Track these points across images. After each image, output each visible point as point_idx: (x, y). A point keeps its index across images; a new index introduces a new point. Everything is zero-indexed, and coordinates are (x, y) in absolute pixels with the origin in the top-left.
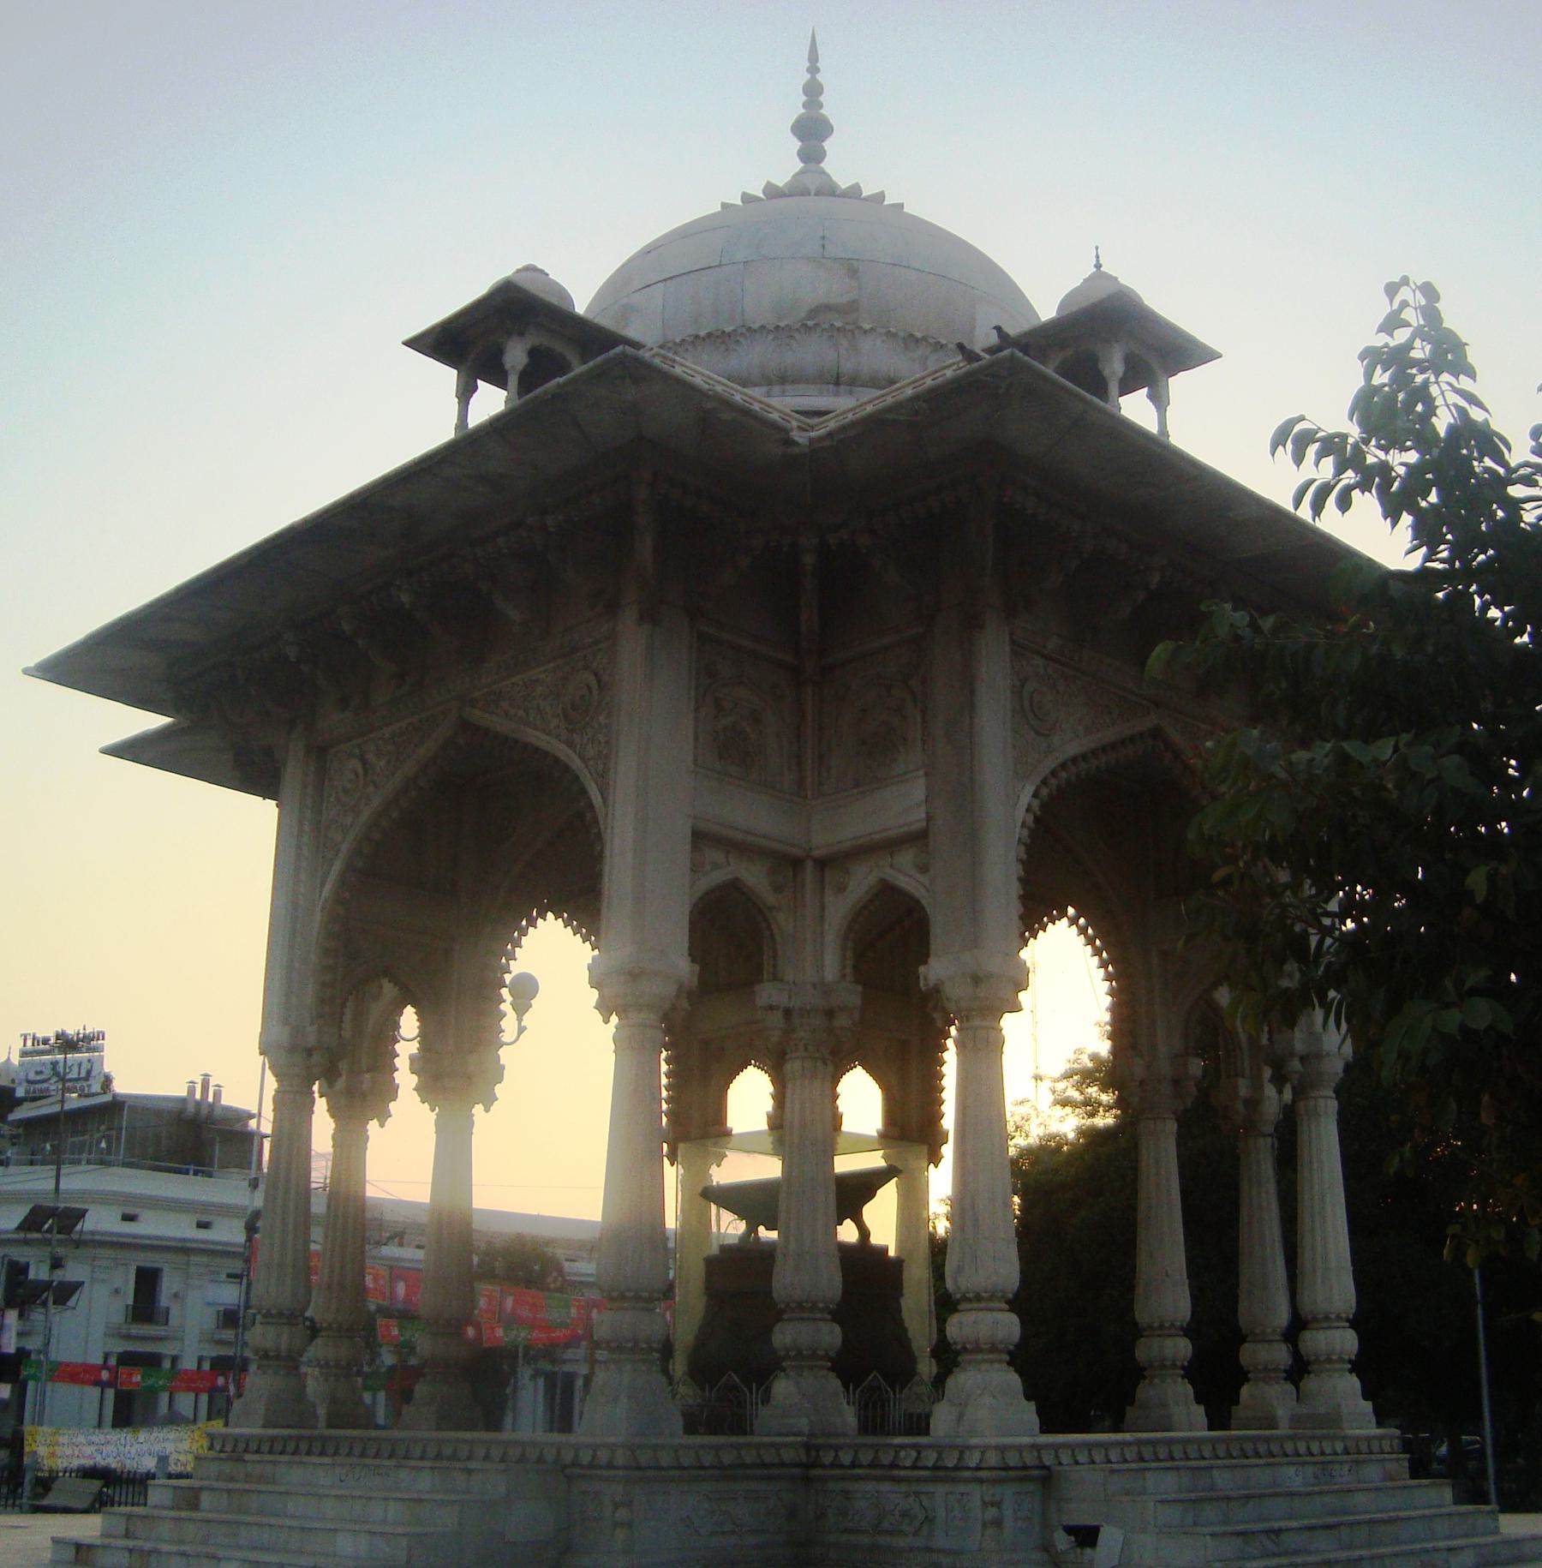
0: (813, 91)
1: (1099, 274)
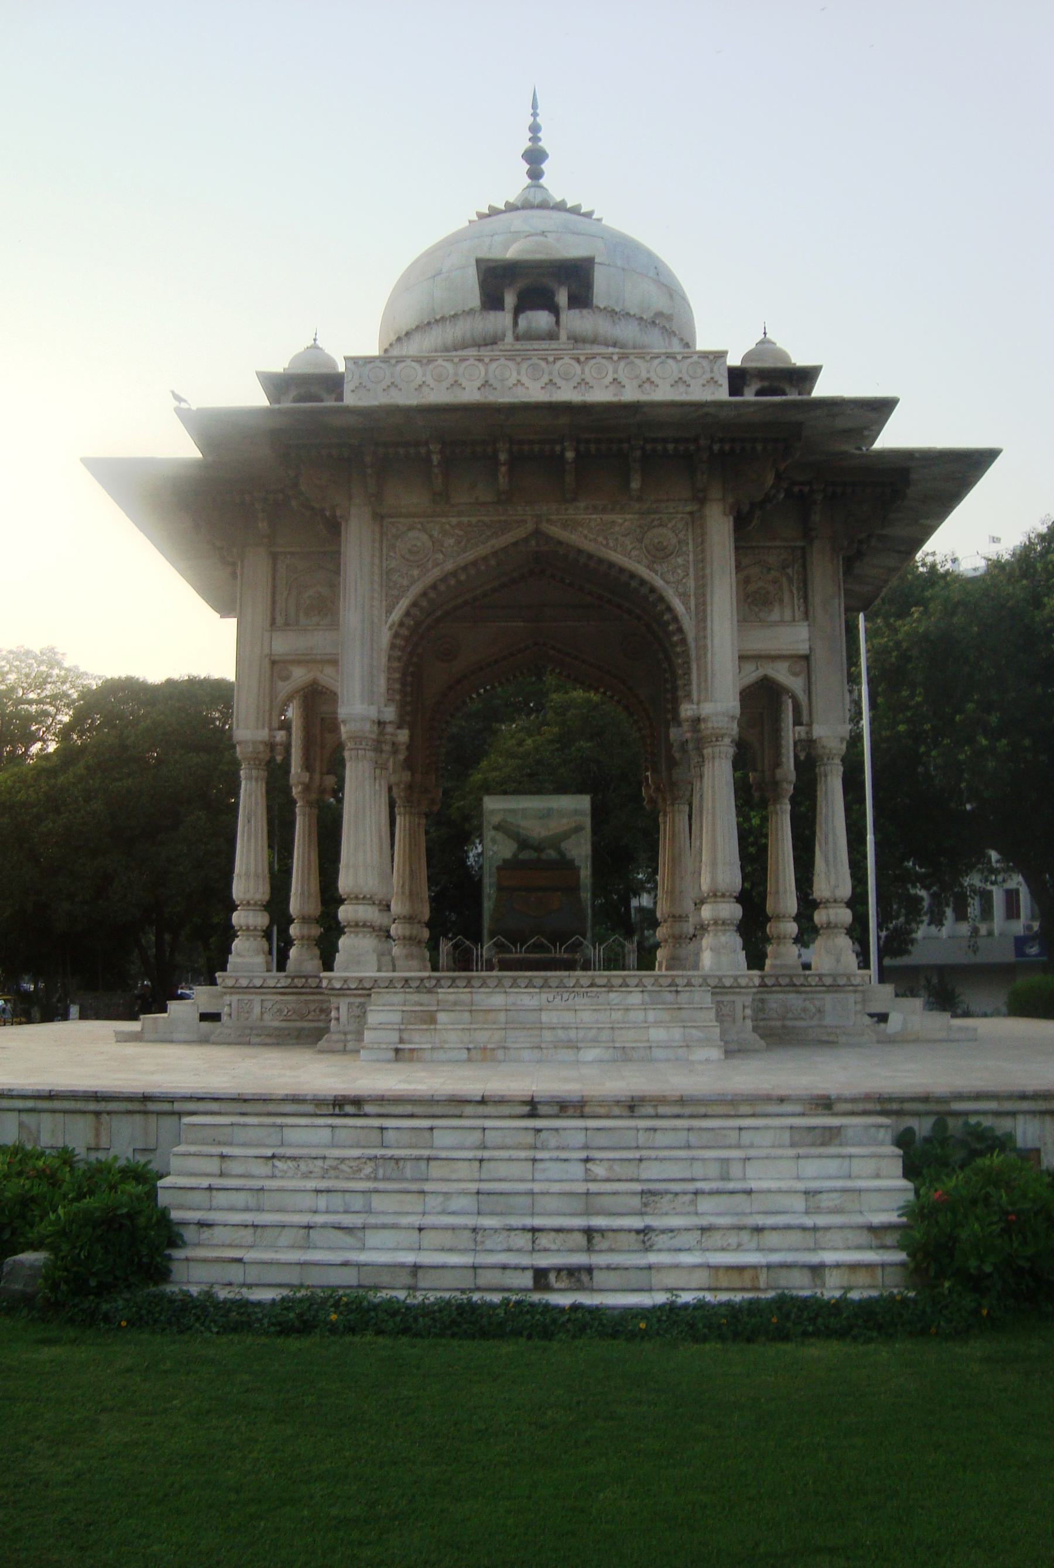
0: (535, 129)
1: (764, 341)
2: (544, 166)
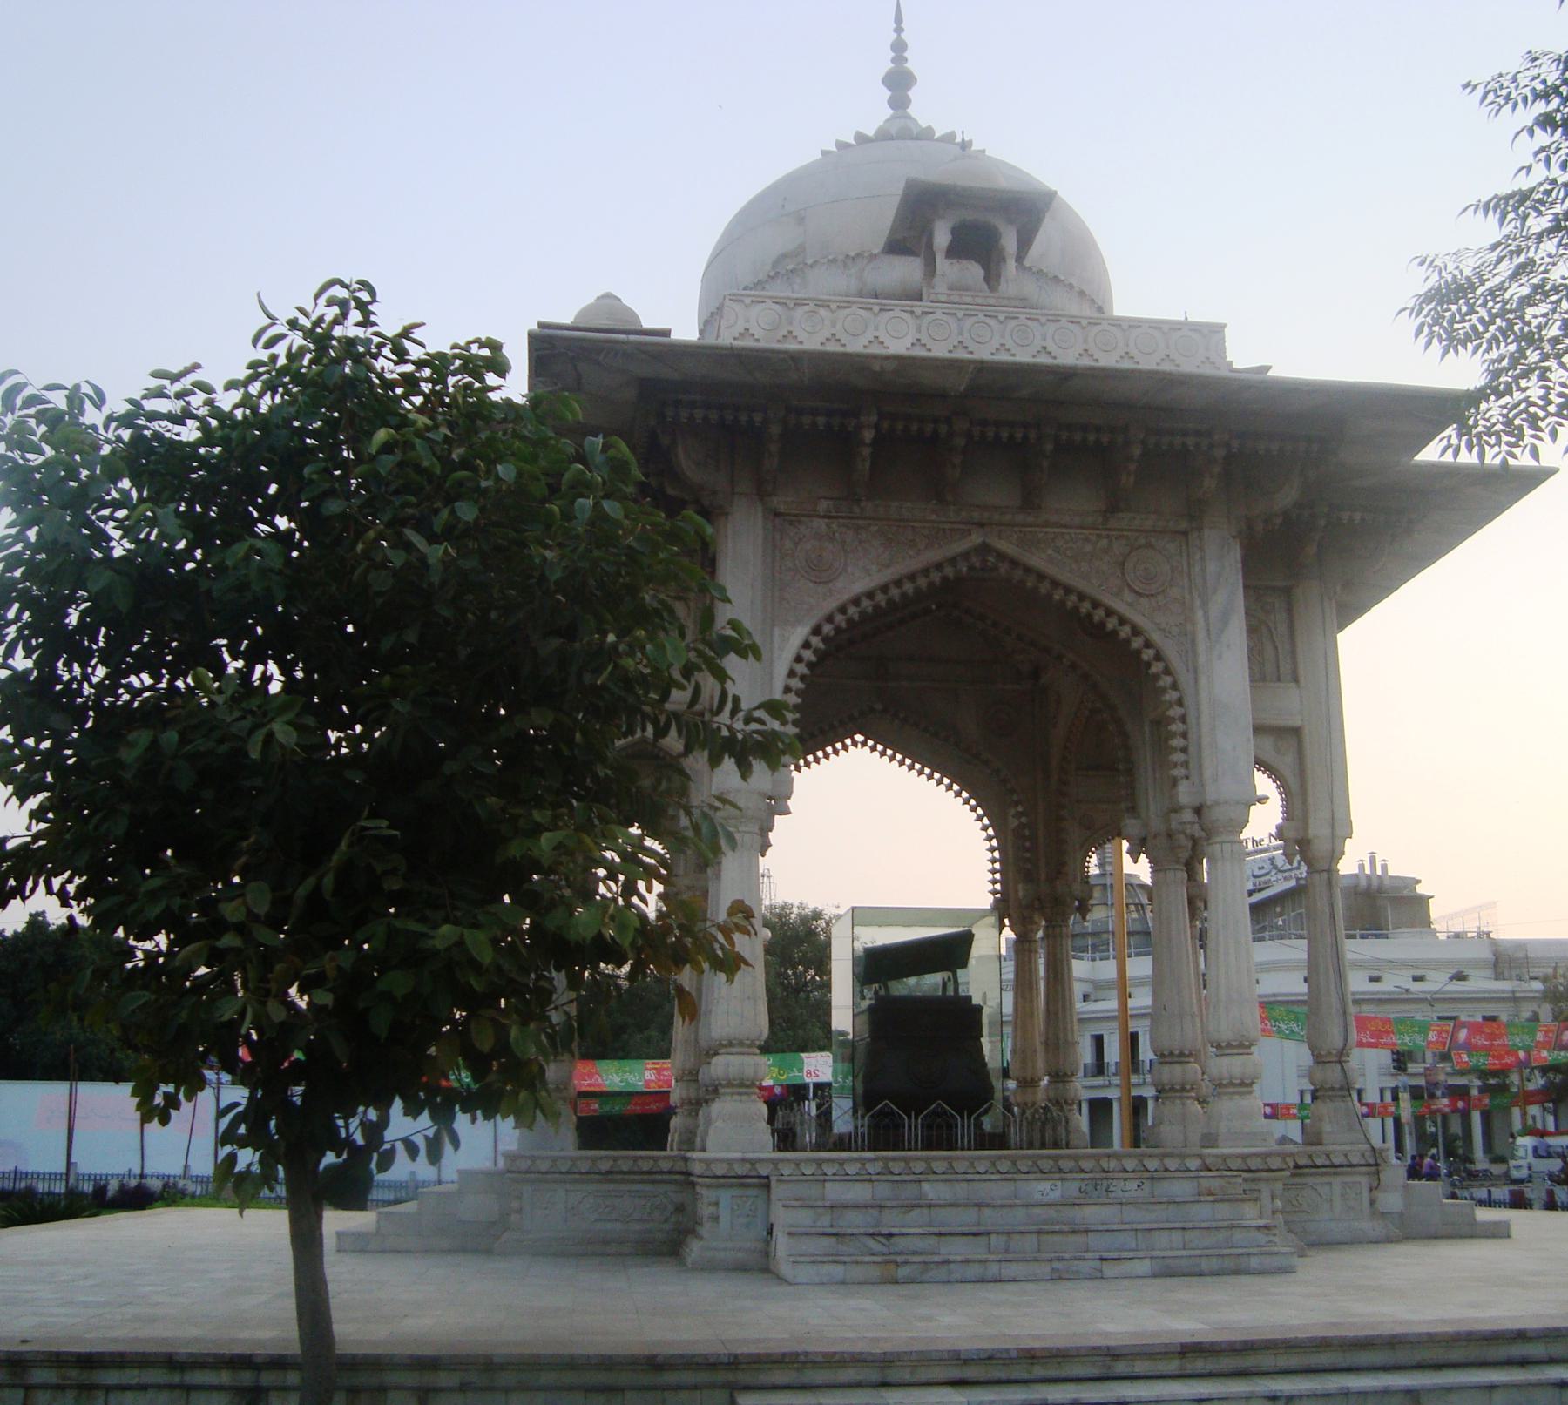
0: (899, 47)
2: (910, 93)
